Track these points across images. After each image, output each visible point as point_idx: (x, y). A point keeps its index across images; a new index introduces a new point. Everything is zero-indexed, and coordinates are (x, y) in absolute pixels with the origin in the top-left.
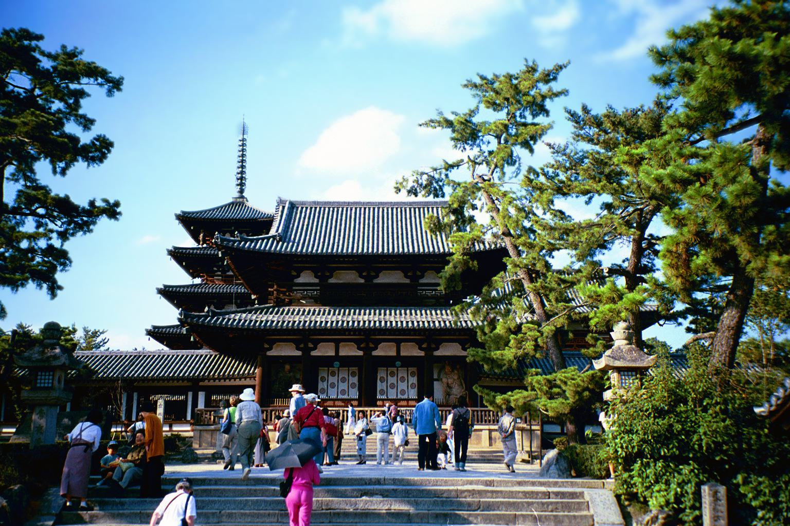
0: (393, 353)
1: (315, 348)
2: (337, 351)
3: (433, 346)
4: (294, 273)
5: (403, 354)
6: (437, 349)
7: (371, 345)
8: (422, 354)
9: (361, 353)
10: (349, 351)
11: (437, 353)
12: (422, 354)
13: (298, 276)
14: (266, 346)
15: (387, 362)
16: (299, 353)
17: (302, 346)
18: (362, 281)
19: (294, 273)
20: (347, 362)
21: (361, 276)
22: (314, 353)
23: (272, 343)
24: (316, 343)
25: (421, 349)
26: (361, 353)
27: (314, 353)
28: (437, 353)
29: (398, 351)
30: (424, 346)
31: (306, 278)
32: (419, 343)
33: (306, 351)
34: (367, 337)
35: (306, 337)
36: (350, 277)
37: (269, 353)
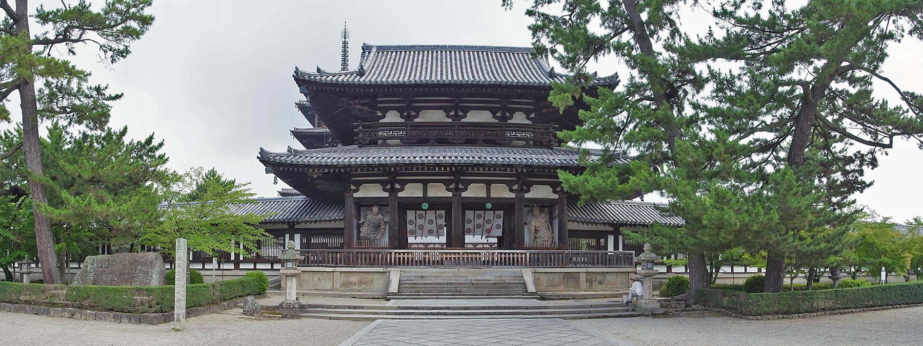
0: (483, 194)
1: (402, 190)
2: (425, 191)
3: (525, 188)
4: (379, 114)
5: (494, 195)
6: (528, 191)
7: (461, 186)
8: (513, 195)
9: (450, 194)
10: (438, 191)
11: (527, 196)
12: (513, 195)
13: (384, 117)
14: (353, 187)
15: (477, 205)
16: (386, 195)
17: (389, 187)
18: (450, 120)
19: (379, 114)
20: (436, 204)
21: (448, 116)
22: (400, 194)
23: (358, 184)
24: (403, 183)
25: (511, 190)
26: (450, 194)
27: (400, 194)
28: (527, 196)
29: (488, 192)
30: (515, 187)
31: (392, 117)
32: (510, 184)
33: (393, 191)
34: (458, 174)
35: (392, 175)
36: (437, 116)
37: (355, 195)
